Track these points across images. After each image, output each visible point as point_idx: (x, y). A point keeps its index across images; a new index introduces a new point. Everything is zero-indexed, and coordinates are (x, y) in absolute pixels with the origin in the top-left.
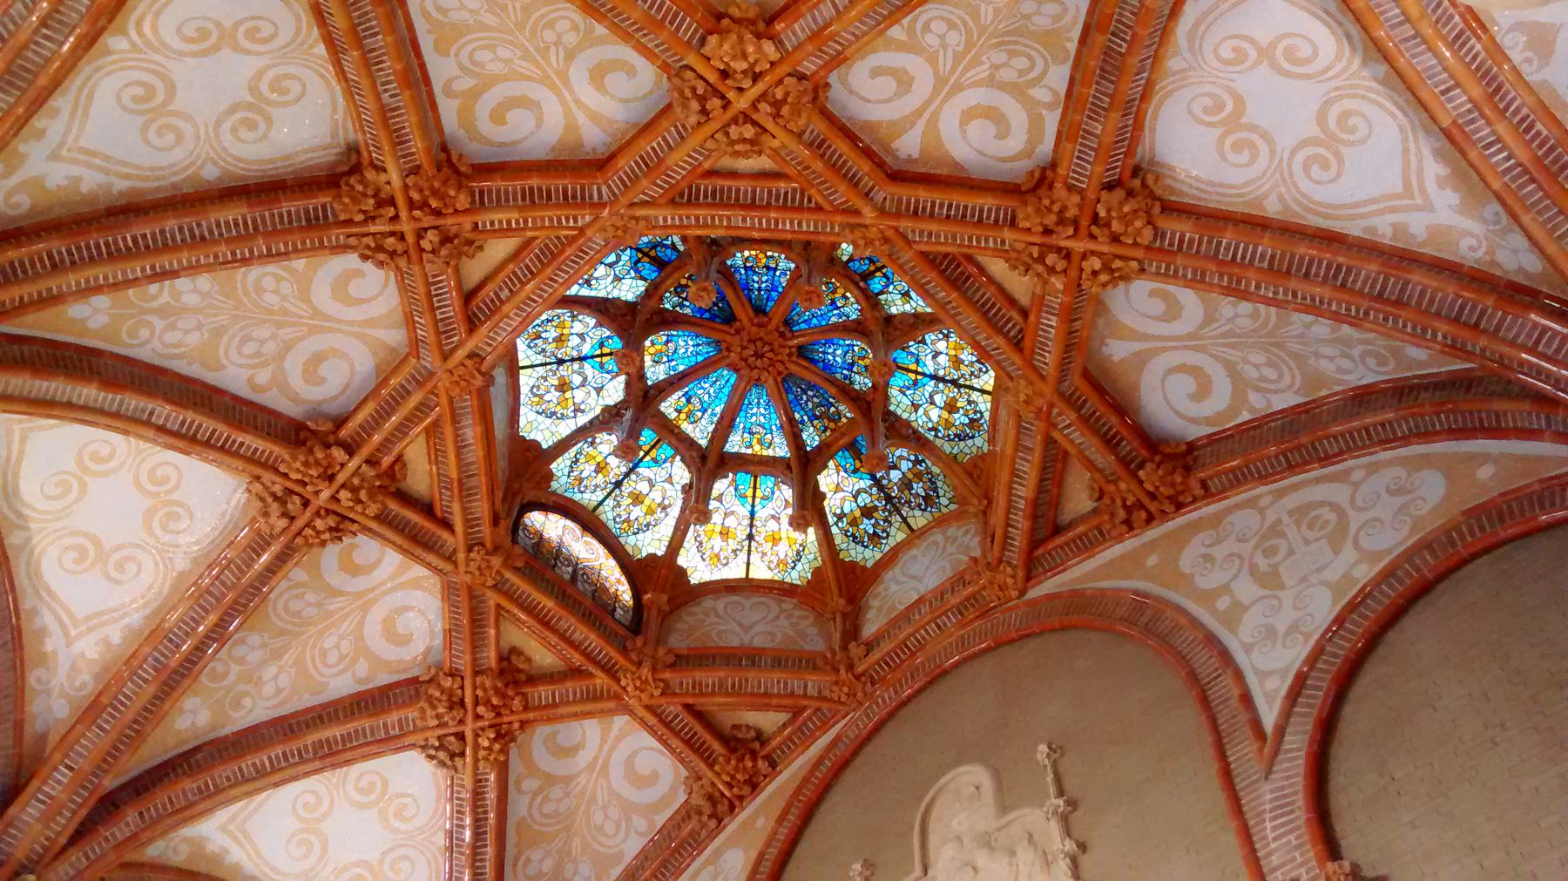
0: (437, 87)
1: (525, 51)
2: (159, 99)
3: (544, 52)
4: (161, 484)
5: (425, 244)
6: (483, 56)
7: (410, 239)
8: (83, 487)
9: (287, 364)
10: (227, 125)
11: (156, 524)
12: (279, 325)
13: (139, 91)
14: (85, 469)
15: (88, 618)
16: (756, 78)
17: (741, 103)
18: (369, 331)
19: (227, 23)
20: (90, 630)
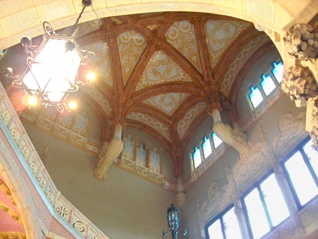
0: (143, 50)
1: (132, 47)
2: (167, 72)
3: (130, 46)
4: (214, 32)
5: (156, 38)
6: (136, 50)
7: (157, 40)
8: (219, 40)
9: (187, 32)
10: (165, 63)
11: (219, 28)
12: (184, 37)
13: (167, 74)
14: (217, 42)
15: (235, 27)
16: (106, 36)
17: (110, 33)
18: (177, 26)
19: (153, 74)
20: (236, 26)
